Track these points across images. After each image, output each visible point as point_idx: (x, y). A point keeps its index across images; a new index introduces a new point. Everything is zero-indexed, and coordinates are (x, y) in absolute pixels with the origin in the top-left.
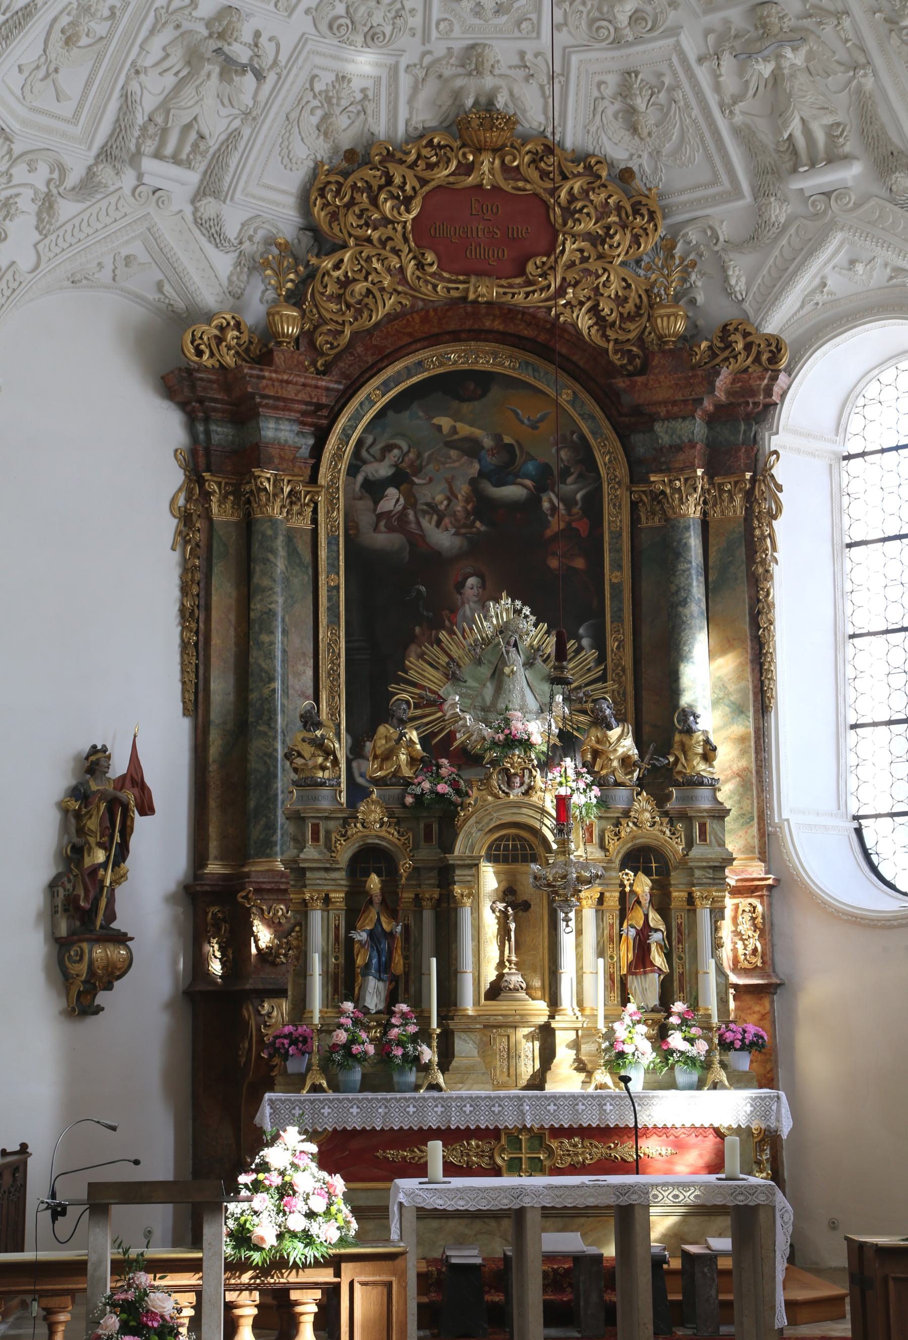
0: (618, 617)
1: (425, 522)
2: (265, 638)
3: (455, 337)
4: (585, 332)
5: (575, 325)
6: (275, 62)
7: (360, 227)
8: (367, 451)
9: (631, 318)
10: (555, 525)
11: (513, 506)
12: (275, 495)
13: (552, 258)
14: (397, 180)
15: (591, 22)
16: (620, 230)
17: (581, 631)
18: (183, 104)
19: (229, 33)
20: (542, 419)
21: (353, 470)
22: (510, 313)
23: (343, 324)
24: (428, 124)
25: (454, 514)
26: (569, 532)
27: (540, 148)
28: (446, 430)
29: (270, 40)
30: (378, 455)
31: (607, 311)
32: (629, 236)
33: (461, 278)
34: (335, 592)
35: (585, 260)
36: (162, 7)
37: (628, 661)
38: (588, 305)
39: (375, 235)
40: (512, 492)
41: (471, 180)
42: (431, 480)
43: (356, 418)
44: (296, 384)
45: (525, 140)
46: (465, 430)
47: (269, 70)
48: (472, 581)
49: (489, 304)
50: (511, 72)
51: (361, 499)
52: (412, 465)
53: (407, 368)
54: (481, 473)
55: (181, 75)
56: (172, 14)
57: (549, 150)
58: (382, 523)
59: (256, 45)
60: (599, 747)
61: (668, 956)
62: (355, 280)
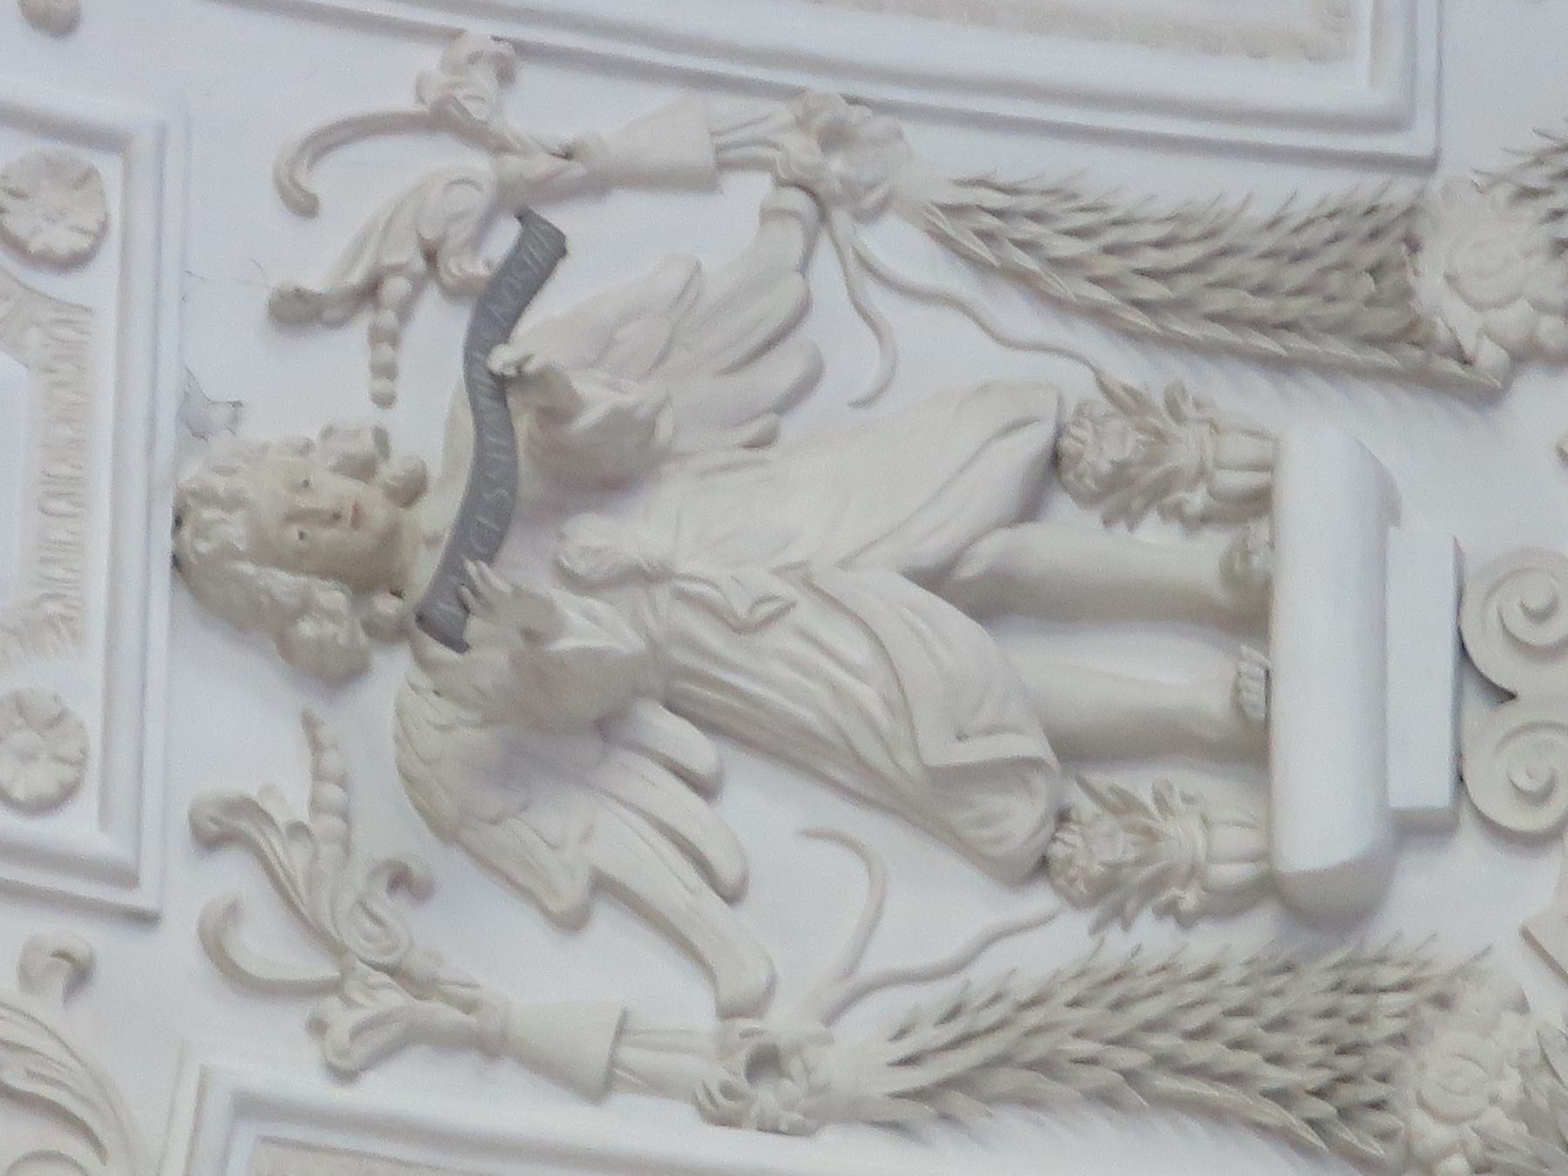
18: (868, 695)
19: (327, 535)
29: (305, 207)
36: (318, 1027)
47: (500, 147)
55: (699, 750)
56: (337, 950)
59: (370, 292)
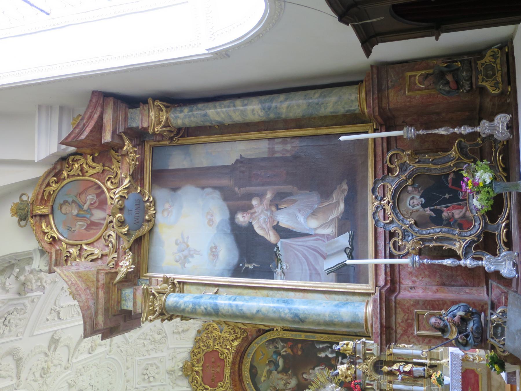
0: (314, 337)
1: (289, 387)
3: (240, 375)
4: (238, 343)
5: (237, 346)
9: (235, 331)
10: (289, 351)
11: (285, 362)
13: (219, 351)
15: (161, 344)
16: (212, 334)
17: (318, 347)
20: (262, 353)
22: (233, 363)
24: (187, 381)
25: (287, 379)
26: (291, 348)
27: (193, 354)
28: (265, 379)
31: (233, 338)
32: (214, 331)
33: (225, 375)
35: (220, 343)
37: (326, 336)
38: (231, 342)
40: (281, 362)
41: (201, 372)
42: (278, 384)
45: (191, 357)
46: (265, 374)
48: (304, 376)
49: (231, 369)
50: (174, 361)
52: (274, 389)
54: (276, 370)
57: (193, 351)
60: (344, 376)
61: (407, 363)
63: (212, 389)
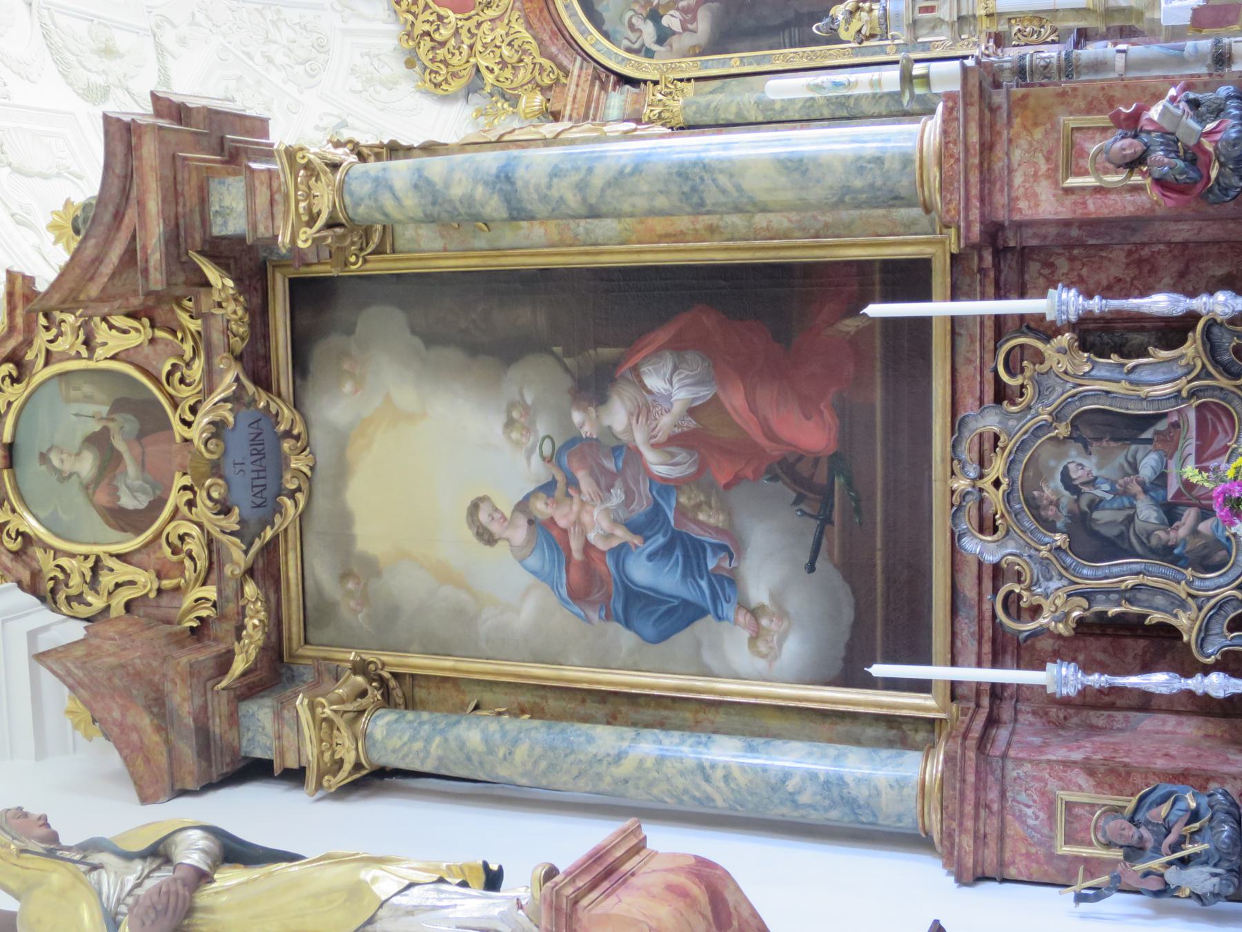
2: (778, 107)
6: (338, 117)
7: (461, 53)
8: (634, 43)
12: (665, 105)
14: (427, 27)
21: (649, 54)
23: (535, 64)
30: (637, 35)
34: (745, 60)
39: (467, 42)
43: (609, 54)
44: (576, 91)
51: (671, 46)
52: (644, 7)
53: (570, 16)
58: (690, 26)
62: (501, 57)
63: (459, 16)
